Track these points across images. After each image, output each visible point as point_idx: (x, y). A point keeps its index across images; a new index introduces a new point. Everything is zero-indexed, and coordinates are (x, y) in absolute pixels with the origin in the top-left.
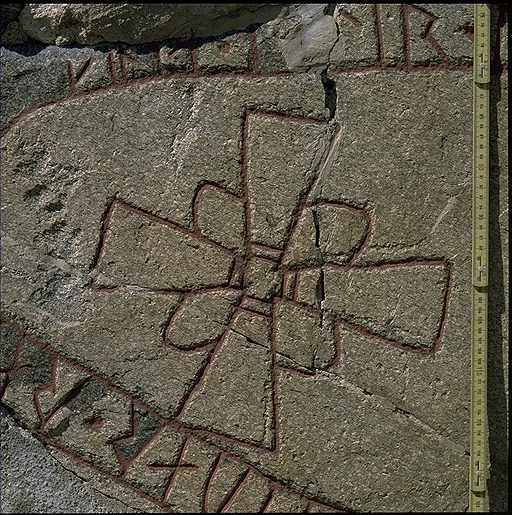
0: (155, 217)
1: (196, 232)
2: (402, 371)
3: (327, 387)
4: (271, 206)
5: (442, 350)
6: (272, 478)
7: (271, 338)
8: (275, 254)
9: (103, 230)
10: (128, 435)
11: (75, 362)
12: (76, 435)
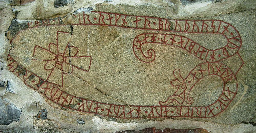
0: (42, 48)
1: (49, 51)
2: (82, 74)
3: (71, 76)
4: (62, 48)
5: (90, 71)
6: (62, 91)
7: (62, 68)
8: (62, 55)
9: (35, 50)
10: (39, 83)
11: (30, 71)
12: (30, 83)
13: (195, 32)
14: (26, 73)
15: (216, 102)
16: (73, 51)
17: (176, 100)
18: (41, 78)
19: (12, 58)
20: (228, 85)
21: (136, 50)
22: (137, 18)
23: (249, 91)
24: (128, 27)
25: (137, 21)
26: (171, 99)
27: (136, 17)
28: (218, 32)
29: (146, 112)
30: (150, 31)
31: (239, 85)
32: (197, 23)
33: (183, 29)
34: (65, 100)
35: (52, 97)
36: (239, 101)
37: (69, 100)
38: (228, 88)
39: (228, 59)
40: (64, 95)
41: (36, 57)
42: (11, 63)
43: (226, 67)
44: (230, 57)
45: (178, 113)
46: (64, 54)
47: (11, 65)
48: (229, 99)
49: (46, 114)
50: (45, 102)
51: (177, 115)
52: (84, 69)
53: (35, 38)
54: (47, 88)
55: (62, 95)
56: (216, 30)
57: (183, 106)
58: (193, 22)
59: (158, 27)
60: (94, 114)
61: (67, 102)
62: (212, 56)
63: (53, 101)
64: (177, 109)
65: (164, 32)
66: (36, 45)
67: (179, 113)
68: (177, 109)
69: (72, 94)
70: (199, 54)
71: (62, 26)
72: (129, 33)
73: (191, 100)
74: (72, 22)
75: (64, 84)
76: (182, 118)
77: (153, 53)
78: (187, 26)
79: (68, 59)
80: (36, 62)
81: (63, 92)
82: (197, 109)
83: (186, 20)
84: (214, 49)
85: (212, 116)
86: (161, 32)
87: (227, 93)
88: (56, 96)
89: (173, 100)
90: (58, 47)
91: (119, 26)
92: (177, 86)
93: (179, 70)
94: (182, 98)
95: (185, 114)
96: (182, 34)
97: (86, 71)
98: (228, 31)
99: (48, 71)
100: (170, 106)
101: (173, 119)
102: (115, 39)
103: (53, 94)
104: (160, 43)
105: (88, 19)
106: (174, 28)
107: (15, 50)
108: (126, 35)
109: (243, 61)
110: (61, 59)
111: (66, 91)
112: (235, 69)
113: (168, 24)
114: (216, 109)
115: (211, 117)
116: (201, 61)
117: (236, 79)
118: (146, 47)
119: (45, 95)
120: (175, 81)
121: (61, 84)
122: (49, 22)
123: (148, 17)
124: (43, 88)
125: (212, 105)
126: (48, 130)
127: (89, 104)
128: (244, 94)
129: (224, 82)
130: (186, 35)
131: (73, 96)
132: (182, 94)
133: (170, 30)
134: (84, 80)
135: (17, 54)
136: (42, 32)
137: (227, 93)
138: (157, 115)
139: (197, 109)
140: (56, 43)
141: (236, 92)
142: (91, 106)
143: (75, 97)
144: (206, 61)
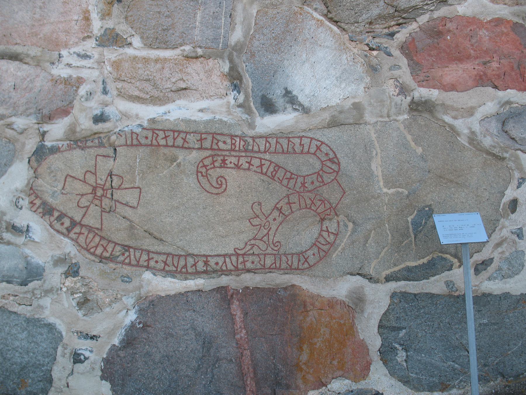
0: (76, 178)
1: (85, 182)
2: (128, 212)
4: (102, 177)
5: (139, 207)
6: (100, 236)
7: (101, 205)
8: (102, 187)
9: (65, 181)
10: (70, 227)
11: (58, 210)
12: (58, 226)
13: (279, 153)
14: (53, 213)
15: (312, 247)
16: (116, 182)
17: (257, 246)
18: (73, 220)
19: (35, 193)
20: (326, 223)
21: (201, 178)
22: (201, 136)
23: (354, 231)
24: (189, 148)
25: (201, 140)
26: (250, 245)
27: (199, 135)
28: (308, 152)
29: (217, 264)
30: (220, 153)
31: (341, 223)
32: (280, 140)
33: (262, 148)
34: (105, 249)
35: (87, 246)
36: (343, 244)
37: (110, 249)
38: (327, 227)
39: (324, 188)
40: (104, 243)
41: (67, 190)
42: (34, 200)
43: (323, 199)
44: (326, 184)
45: (261, 264)
46: (104, 185)
47: (34, 202)
48: (329, 243)
49: (78, 269)
50: (77, 252)
51: (259, 266)
52: (131, 205)
53: (66, 165)
54: (80, 233)
55: (101, 243)
56: (306, 149)
57: (267, 254)
58: (275, 139)
59: (229, 147)
60: (144, 269)
61: (107, 252)
62: (303, 184)
63: (88, 251)
64: (260, 258)
65: (237, 154)
66: (68, 175)
67: (263, 263)
68: (260, 258)
69: (114, 240)
70: (285, 182)
71: (103, 148)
72: (191, 156)
73: (278, 245)
74: (116, 143)
75: (103, 227)
76: (267, 270)
77: (224, 181)
78: (268, 145)
79: (109, 192)
80: (66, 197)
81: (102, 238)
82: (287, 258)
83: (266, 138)
84: (304, 174)
85: (308, 266)
86: (233, 153)
87: (325, 234)
88: (93, 244)
89: (253, 245)
90: (96, 177)
91: (178, 147)
92: (257, 225)
93: (260, 204)
94: (265, 242)
95: (271, 266)
96: (261, 156)
97: (134, 208)
98: (321, 151)
99: (82, 209)
100: (249, 255)
101: (254, 272)
102: (172, 164)
103: (88, 241)
104: (232, 168)
105: (137, 138)
106: (250, 148)
107: (40, 181)
108: (187, 158)
109: (343, 190)
110: (99, 193)
111: (106, 237)
112: (334, 200)
113: (242, 143)
114: (312, 256)
115: (306, 269)
116: (288, 191)
117: (336, 214)
118: (214, 173)
119: (77, 242)
120: (255, 219)
121: (99, 227)
122: (86, 144)
123: (216, 134)
124: (75, 233)
125: (306, 251)
126: (80, 292)
127: (138, 254)
128: (349, 234)
129: (321, 219)
130: (267, 156)
131: (116, 244)
132: (265, 238)
133: (246, 151)
134: (131, 221)
135: (41, 186)
136: (76, 156)
137: (325, 234)
138: (232, 268)
139: (287, 258)
140: (93, 171)
141: (338, 233)
142: (140, 257)
143: (119, 244)
144: (295, 190)
